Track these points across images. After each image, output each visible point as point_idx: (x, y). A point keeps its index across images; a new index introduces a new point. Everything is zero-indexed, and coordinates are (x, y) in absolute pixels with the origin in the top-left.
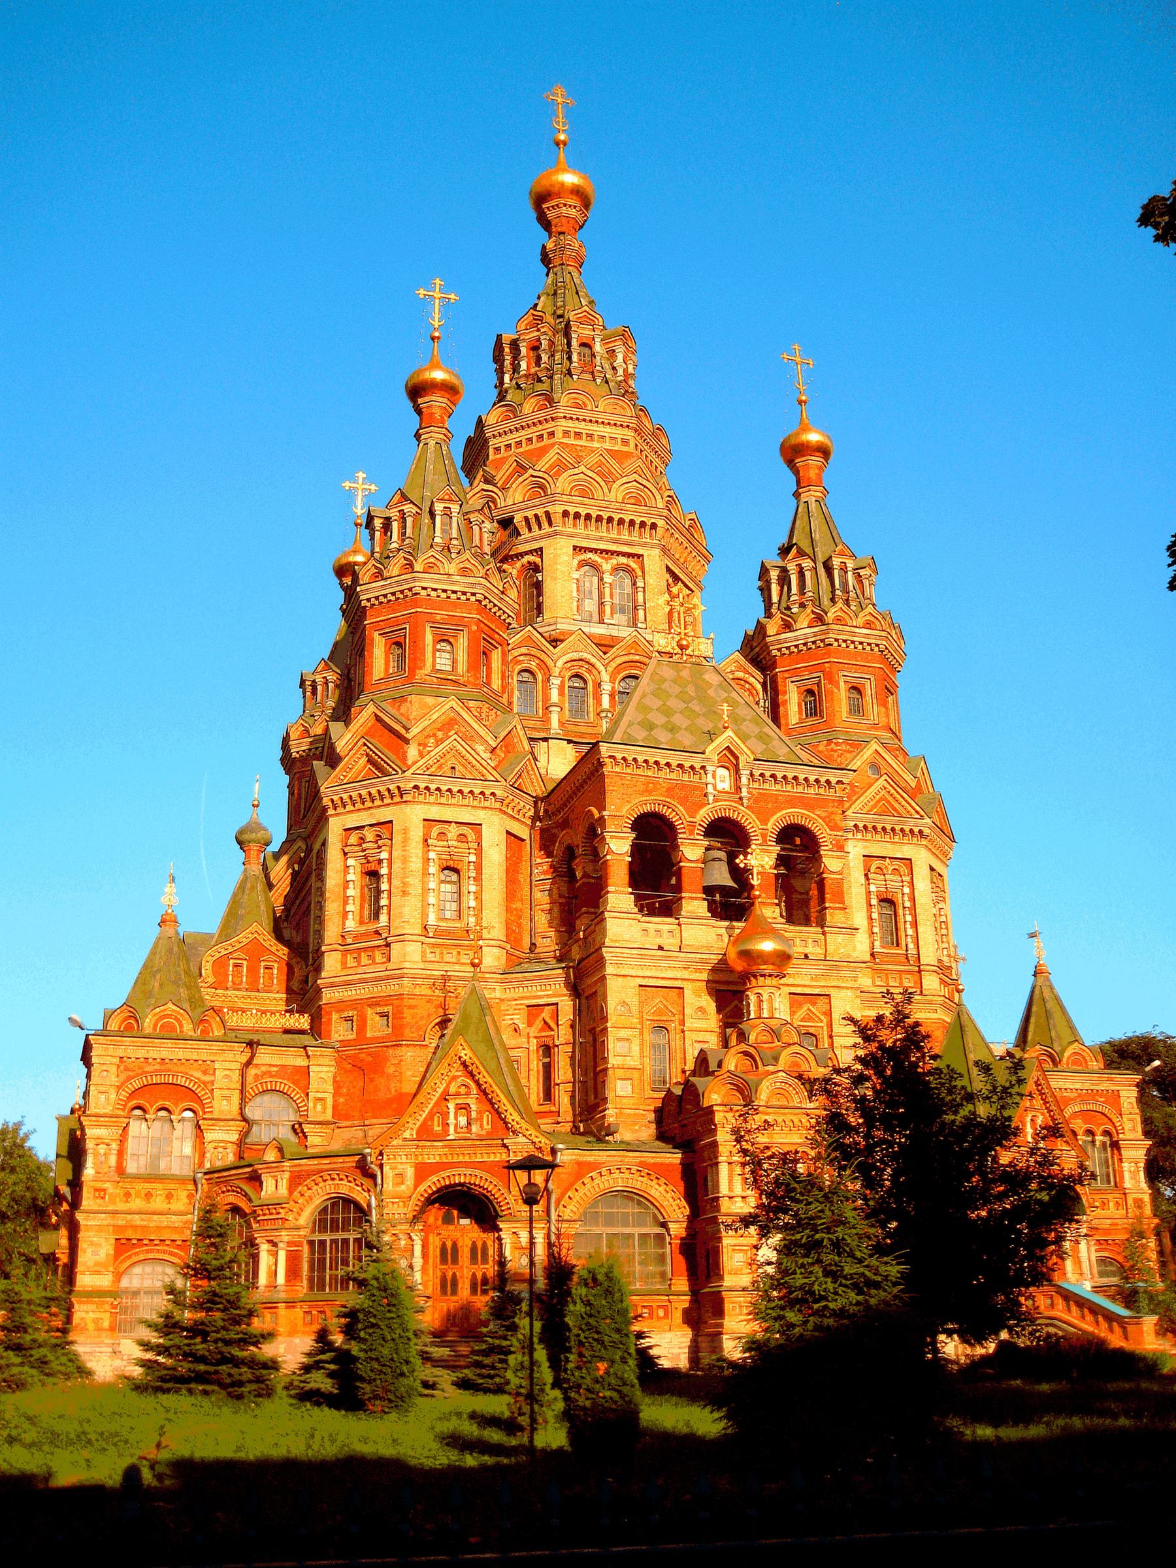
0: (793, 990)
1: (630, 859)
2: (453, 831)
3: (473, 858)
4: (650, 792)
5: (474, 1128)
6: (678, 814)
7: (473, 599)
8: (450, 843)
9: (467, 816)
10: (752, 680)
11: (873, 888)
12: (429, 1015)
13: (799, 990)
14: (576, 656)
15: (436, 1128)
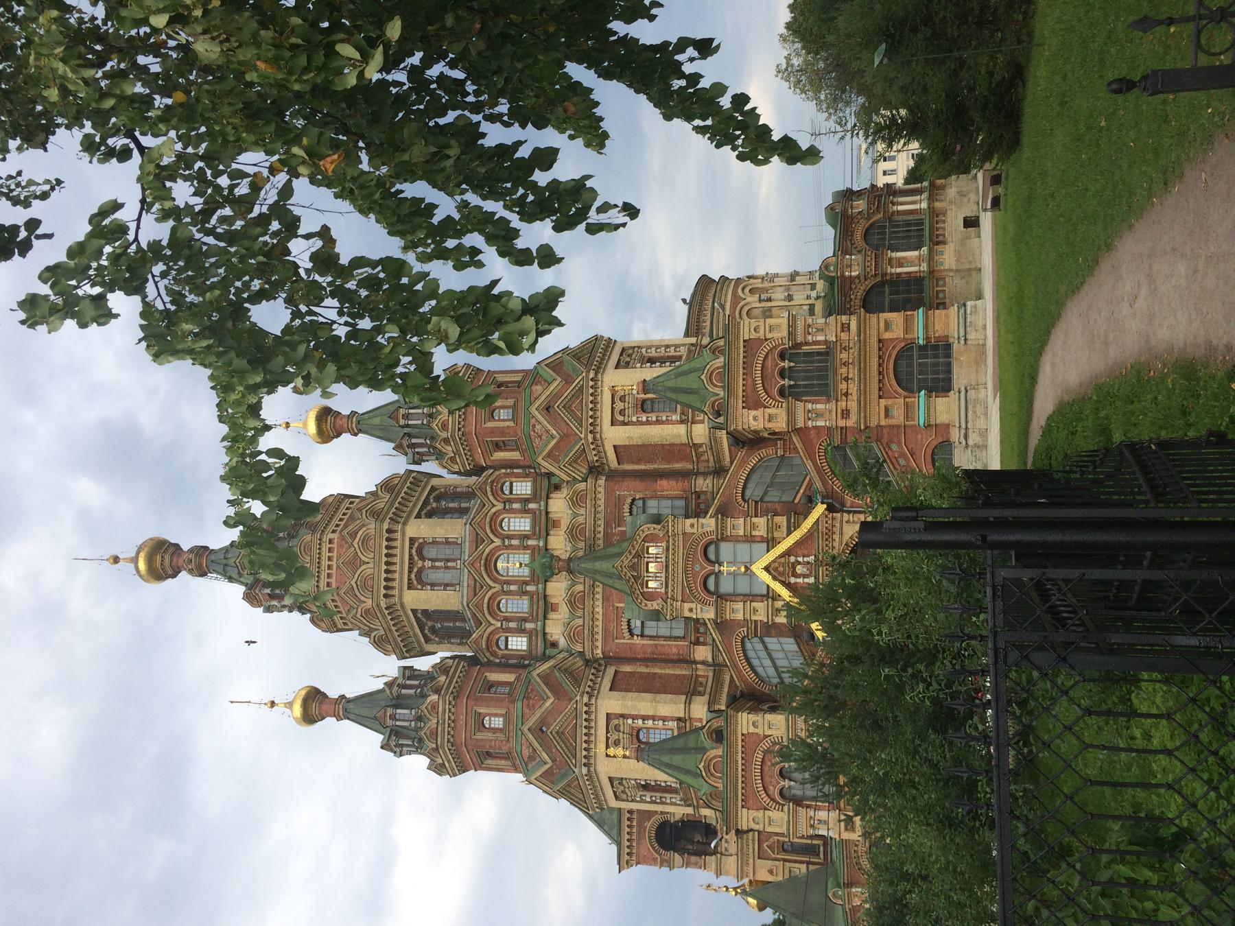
3: (630, 721)
11: (634, 419)
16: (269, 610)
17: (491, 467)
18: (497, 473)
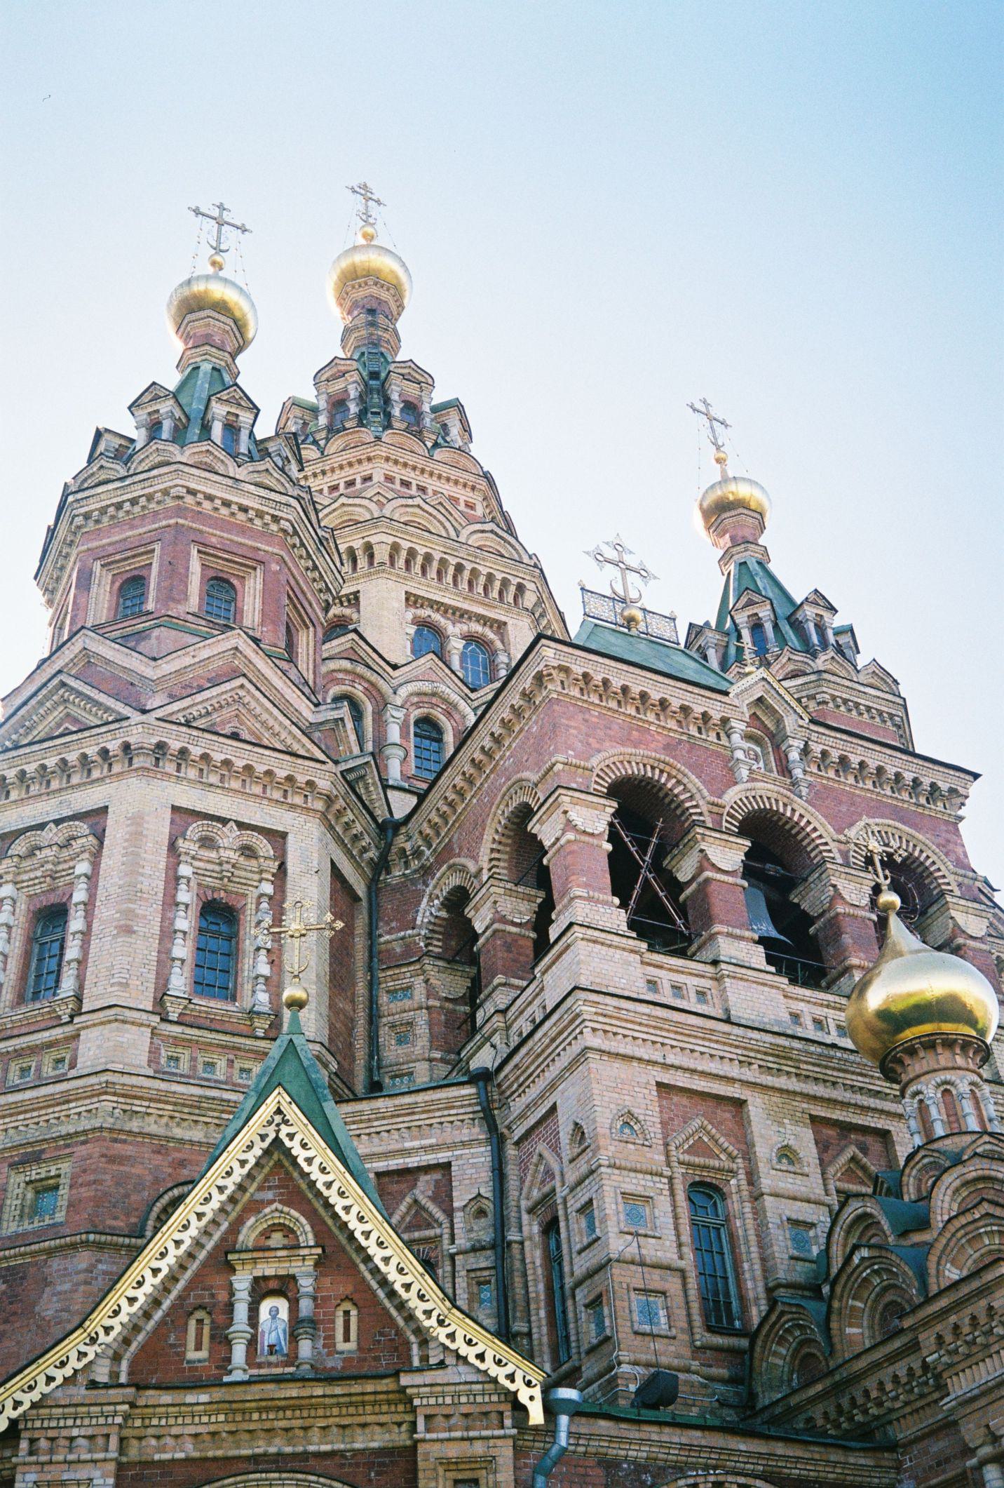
1: (609, 847)
2: (229, 838)
3: (268, 888)
5: (305, 1348)
6: (693, 790)
7: (274, 527)
8: (225, 854)
12: (156, 1181)
14: (427, 687)
15: (192, 1355)
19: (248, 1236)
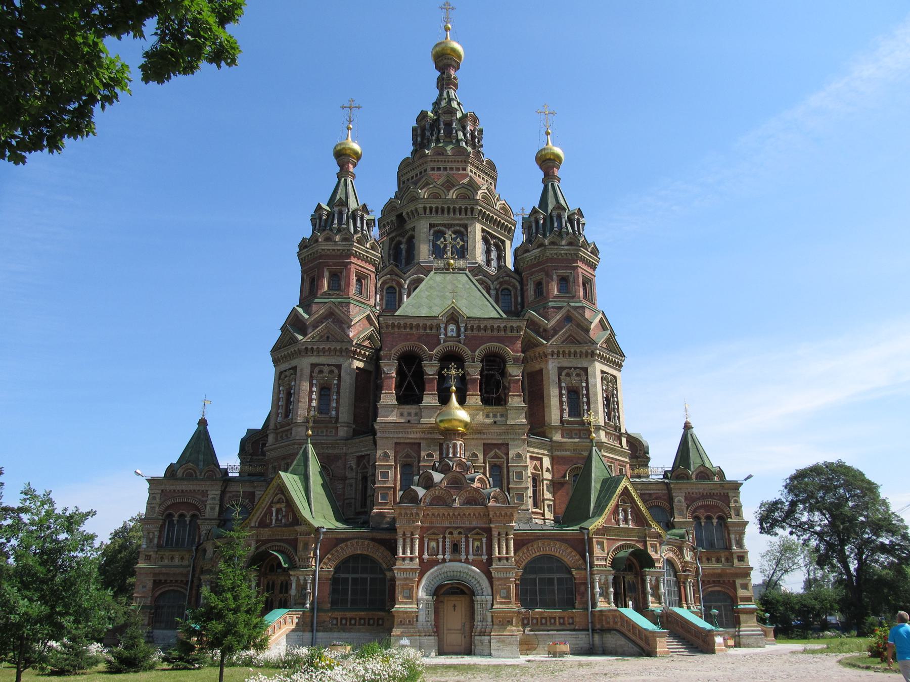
0: (486, 442)
2: (326, 369)
3: (335, 382)
4: (408, 340)
9: (334, 361)
10: (513, 280)
13: (489, 442)
16: (414, 129)
17: (522, 279)
18: (517, 284)
19: (276, 499)
